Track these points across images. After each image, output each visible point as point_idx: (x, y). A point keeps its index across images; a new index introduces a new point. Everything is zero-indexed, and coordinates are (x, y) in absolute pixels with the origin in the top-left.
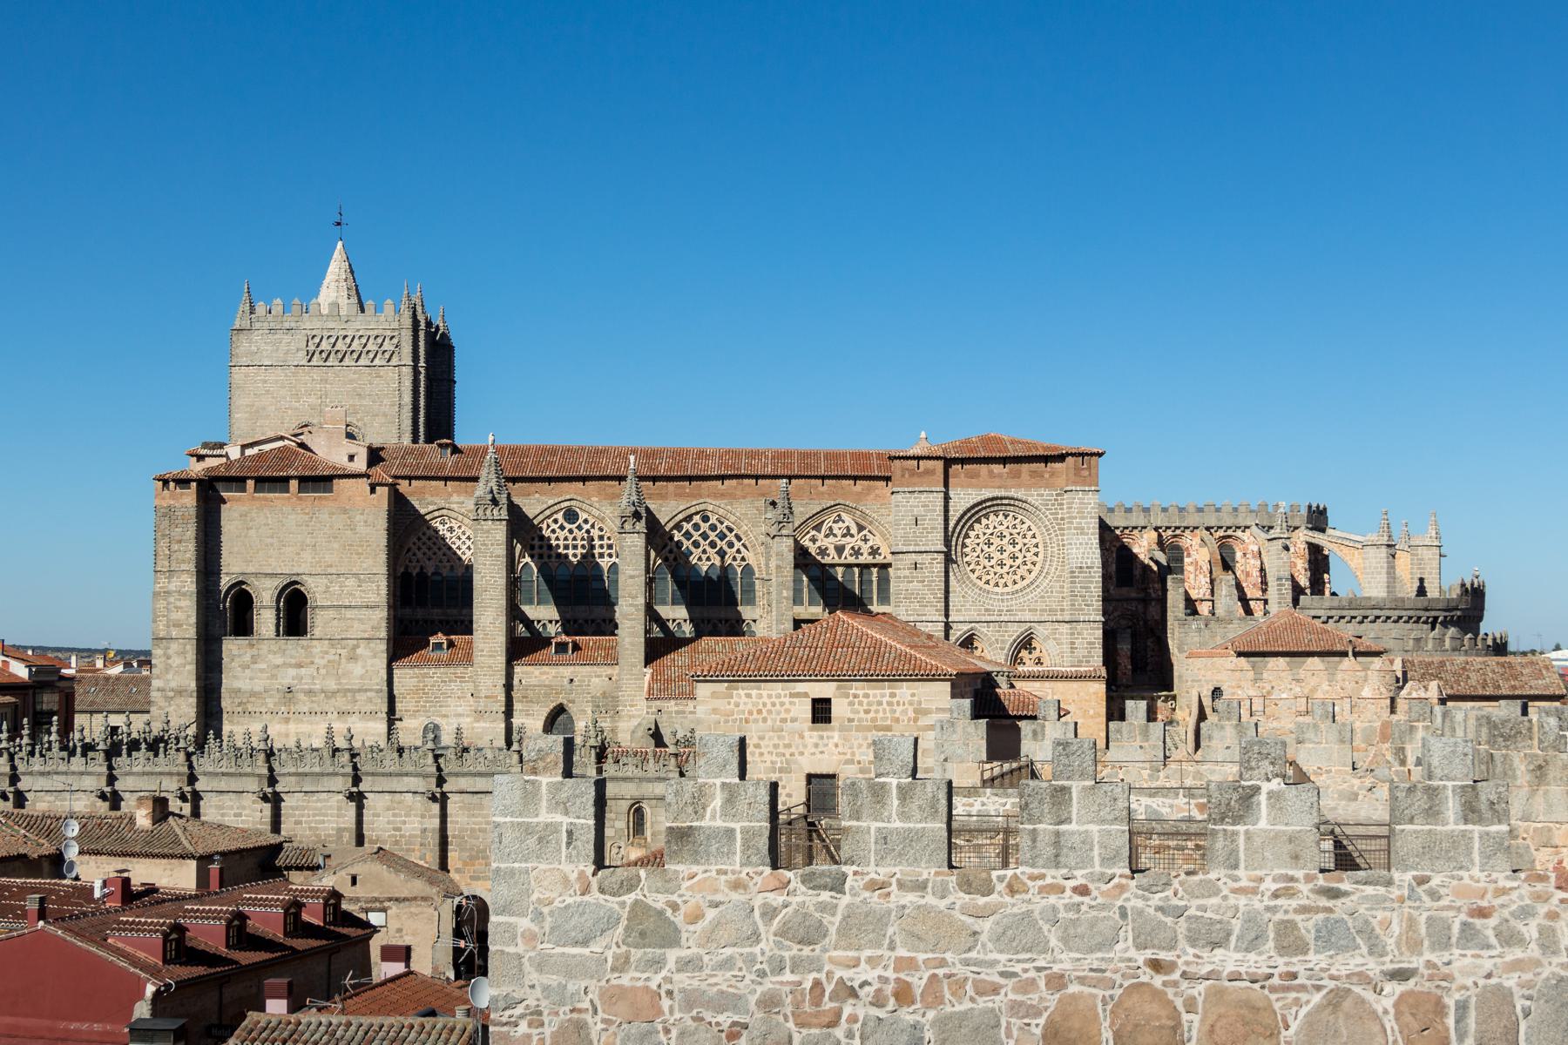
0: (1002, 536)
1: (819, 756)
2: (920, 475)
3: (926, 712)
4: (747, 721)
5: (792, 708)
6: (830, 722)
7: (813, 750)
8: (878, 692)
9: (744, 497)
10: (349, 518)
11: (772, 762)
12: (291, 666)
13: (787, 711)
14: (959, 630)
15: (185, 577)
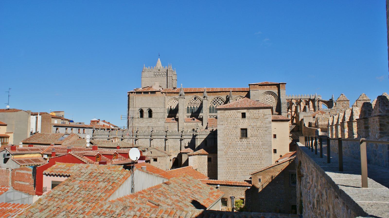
0: (269, 98)
1: (243, 125)
2: (255, 88)
3: (266, 115)
4: (228, 118)
5: (237, 115)
6: (245, 118)
7: (242, 123)
8: (256, 111)
9: (224, 95)
10: (158, 98)
11: (233, 126)
12: (149, 122)
13: (236, 115)
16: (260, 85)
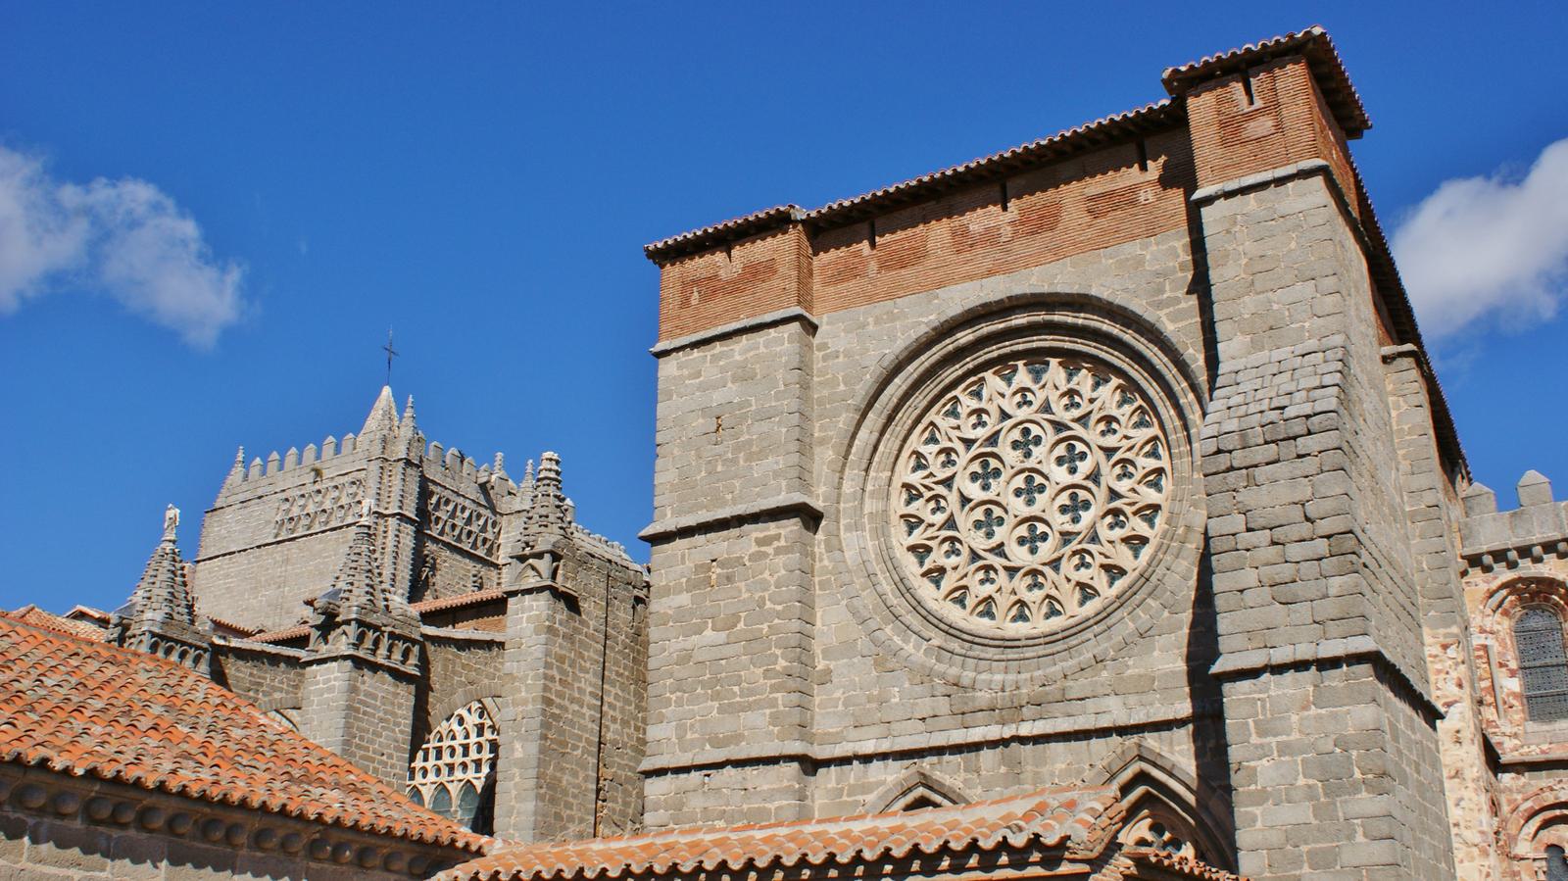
0: (1026, 443)
14: (866, 789)
16: (826, 231)
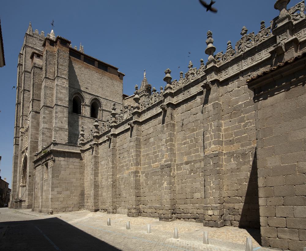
15: (64, 80)
